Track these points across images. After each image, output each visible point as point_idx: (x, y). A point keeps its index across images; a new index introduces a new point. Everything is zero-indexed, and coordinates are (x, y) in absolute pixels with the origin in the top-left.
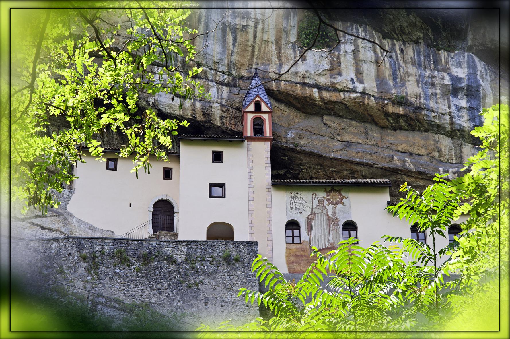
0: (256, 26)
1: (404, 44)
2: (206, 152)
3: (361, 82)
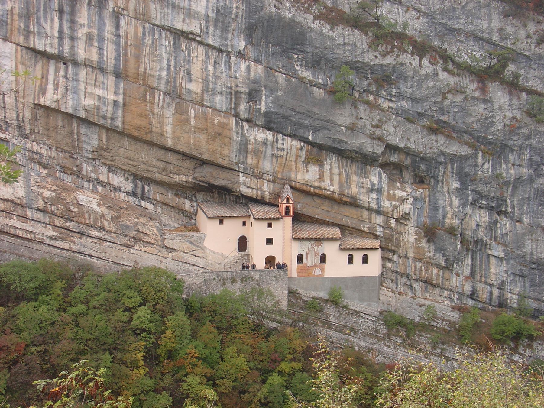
2: (266, 224)
3: (333, 186)
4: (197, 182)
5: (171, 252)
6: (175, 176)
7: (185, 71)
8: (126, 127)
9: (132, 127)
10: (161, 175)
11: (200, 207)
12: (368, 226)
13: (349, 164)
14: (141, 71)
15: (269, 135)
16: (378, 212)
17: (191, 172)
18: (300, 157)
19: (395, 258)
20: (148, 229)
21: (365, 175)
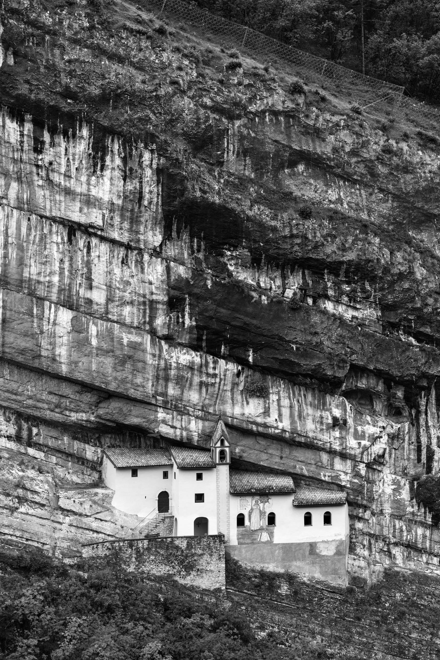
0: (220, 383)
1: (306, 390)
2: (193, 475)
3: (281, 421)
4: (101, 421)
5: (67, 516)
6: (73, 414)
7: (84, 276)
8: (7, 350)
9: (14, 351)
10: (53, 413)
11: (106, 454)
12: (330, 474)
13: (302, 393)
14: (26, 277)
15: (195, 358)
16: (344, 456)
17: (93, 408)
18: (238, 384)
19: (367, 515)
20: (37, 485)
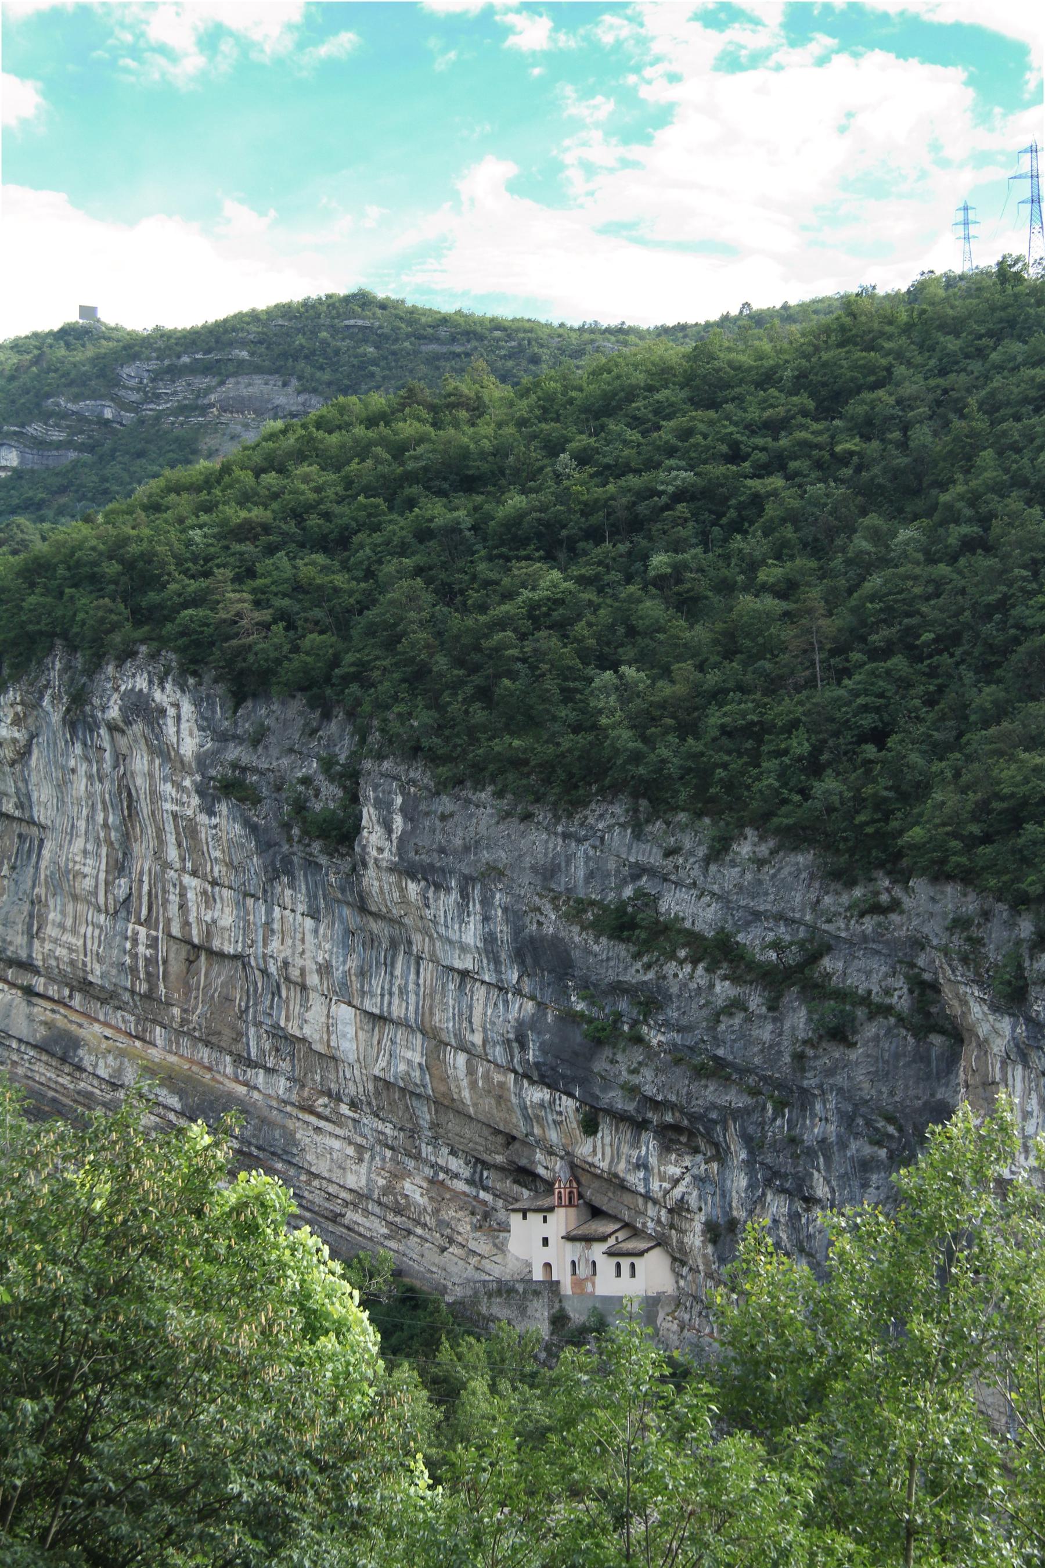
2: (540, 1217)
21: (636, 1144)
